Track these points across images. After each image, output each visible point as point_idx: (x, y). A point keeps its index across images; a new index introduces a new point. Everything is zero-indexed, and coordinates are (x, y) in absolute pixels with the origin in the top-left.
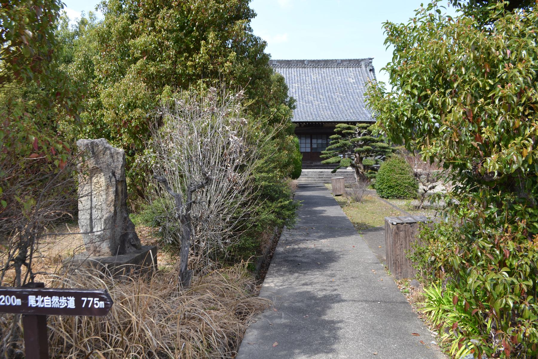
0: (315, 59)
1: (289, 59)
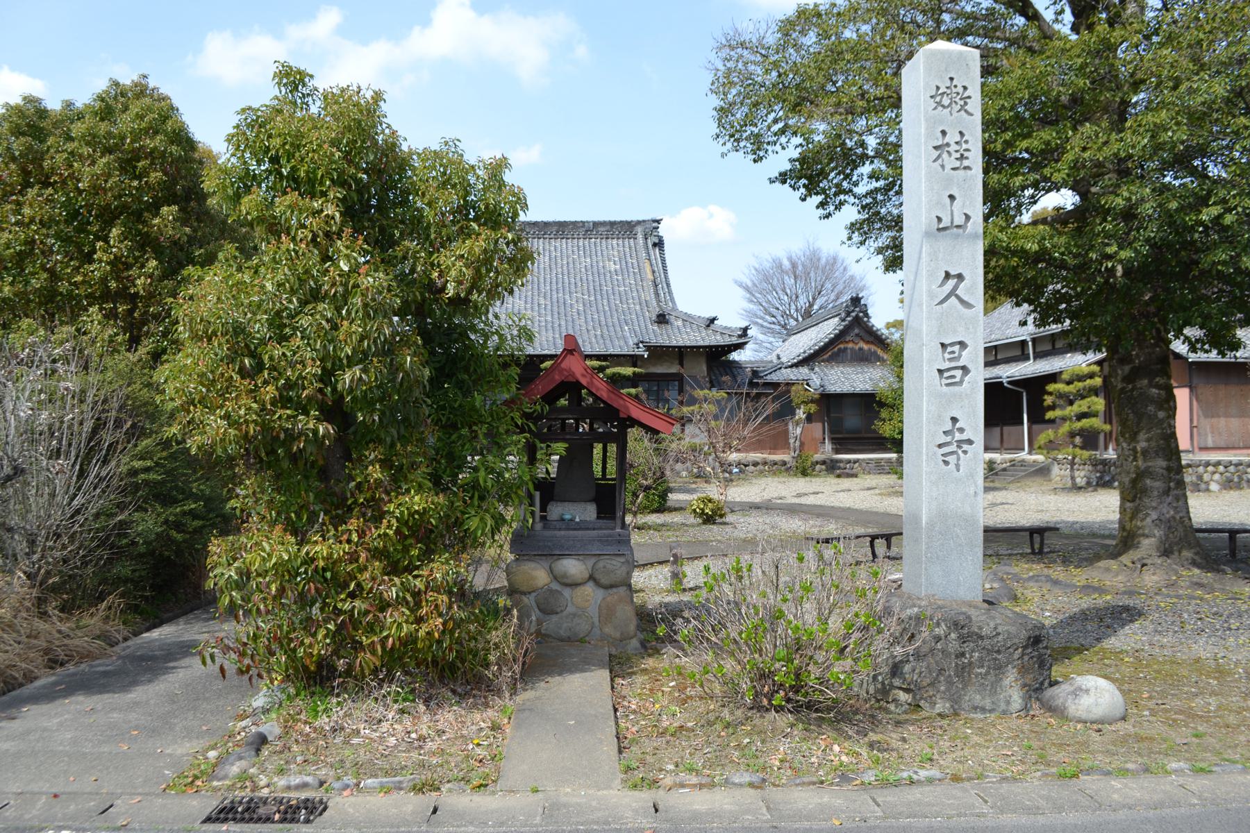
0: (539, 220)
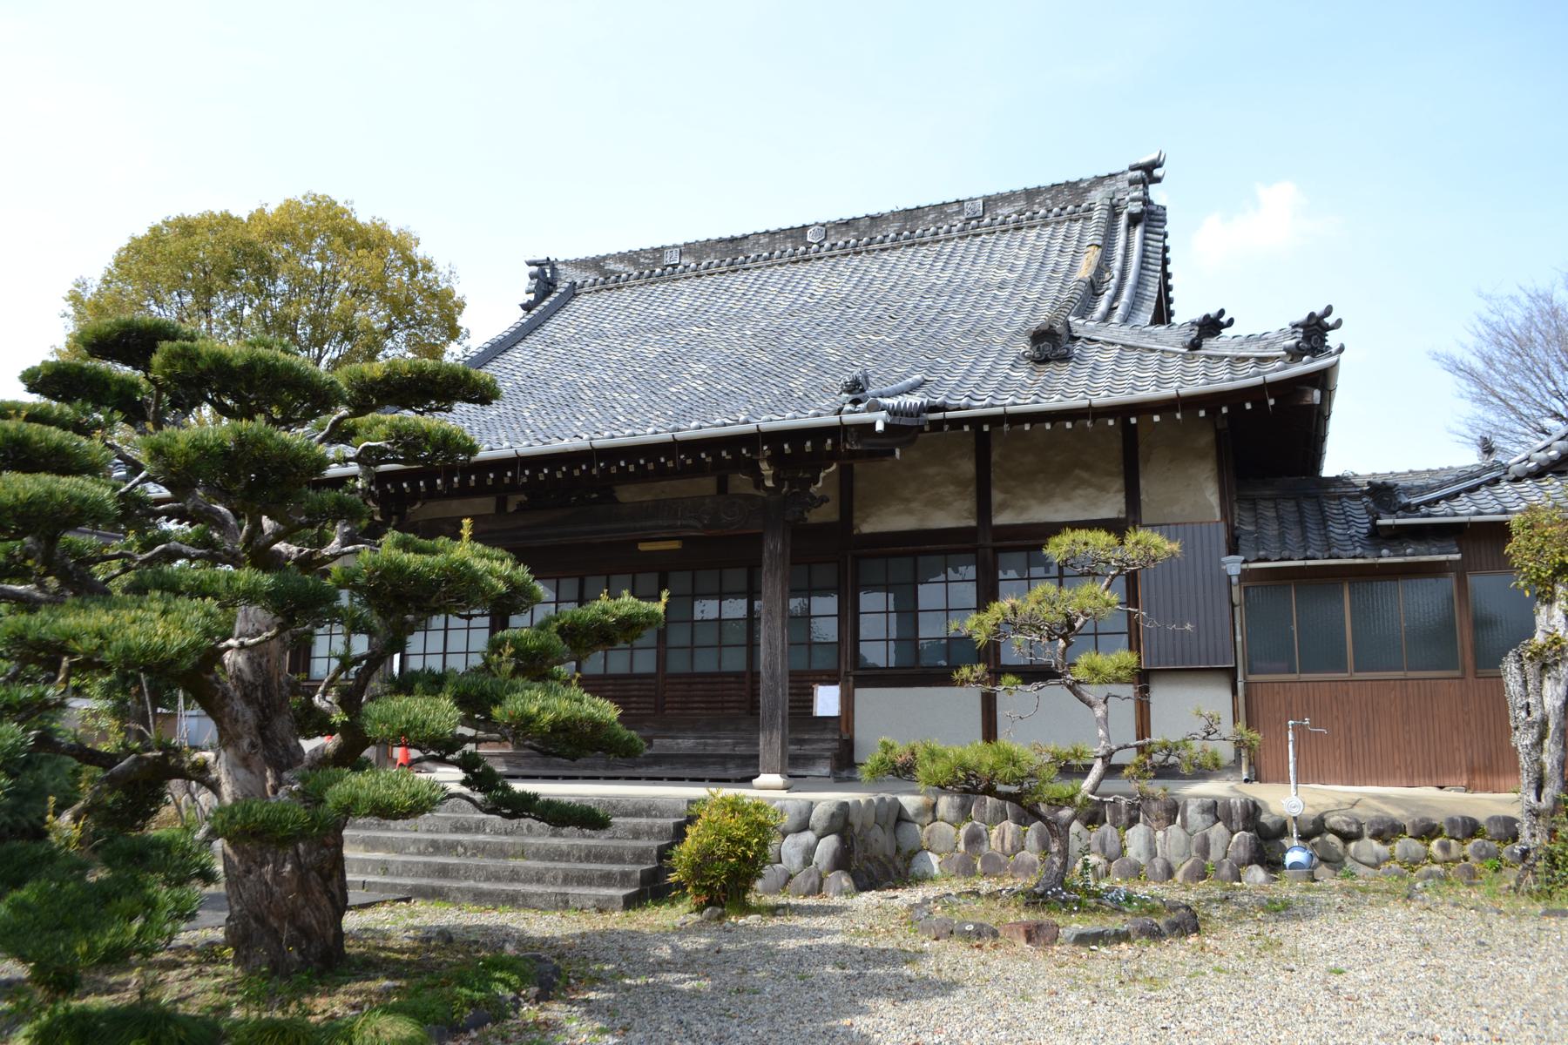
1: (738, 234)
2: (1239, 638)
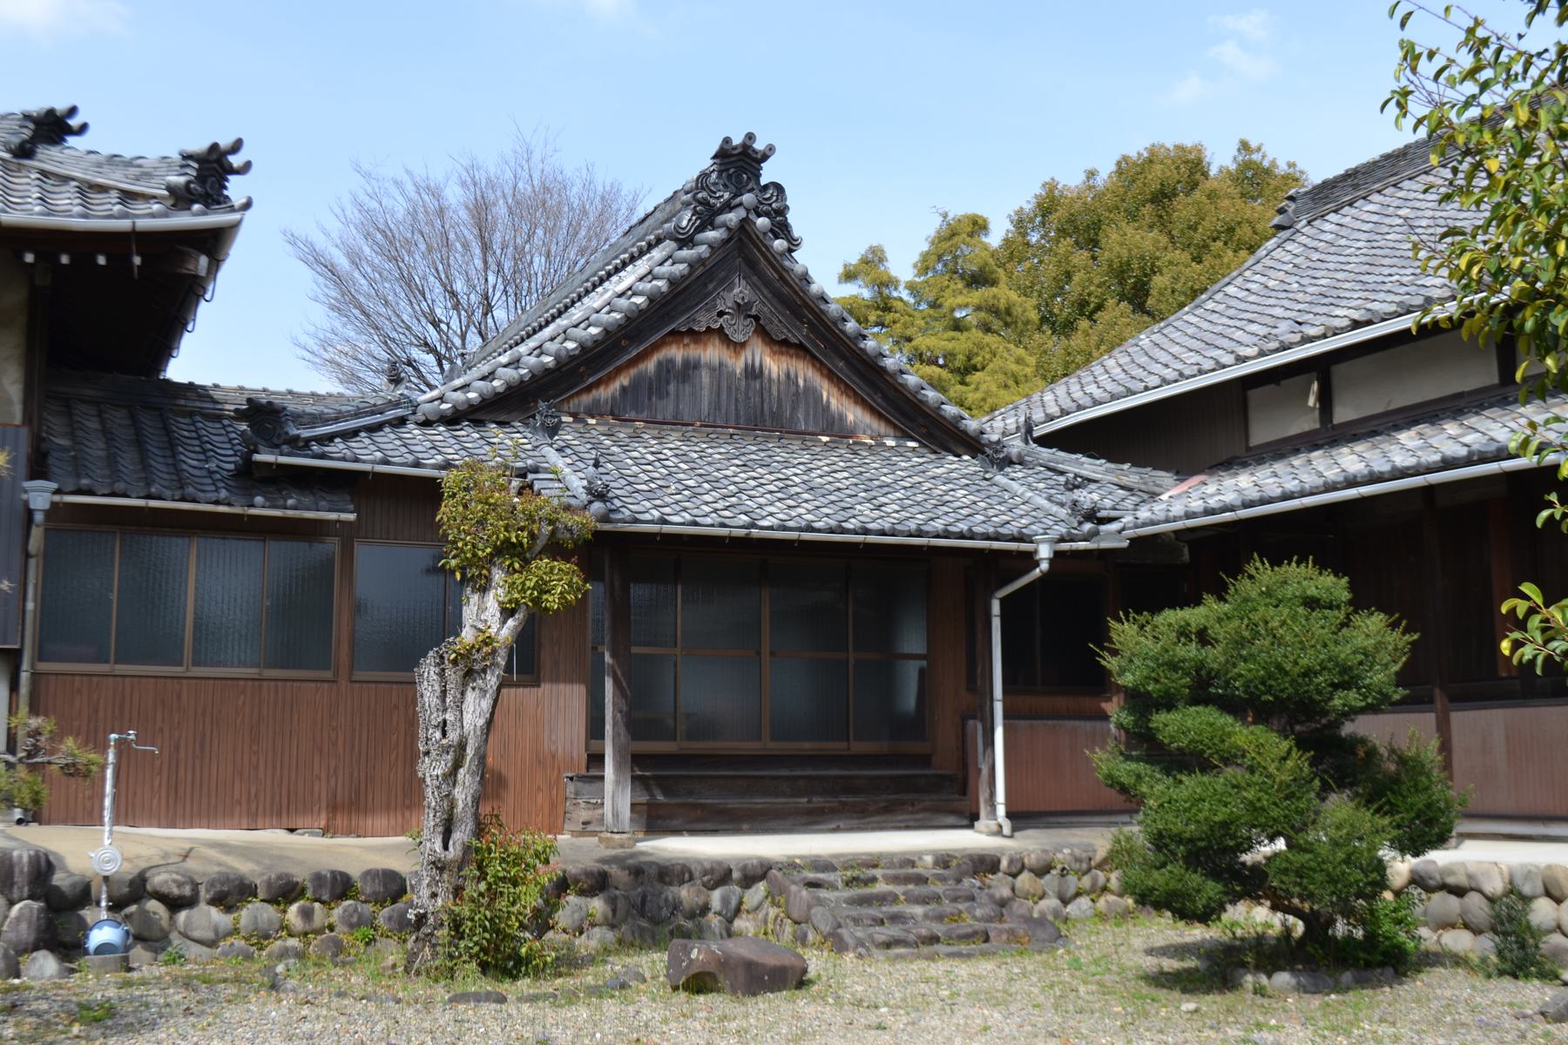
2: (30, 606)
